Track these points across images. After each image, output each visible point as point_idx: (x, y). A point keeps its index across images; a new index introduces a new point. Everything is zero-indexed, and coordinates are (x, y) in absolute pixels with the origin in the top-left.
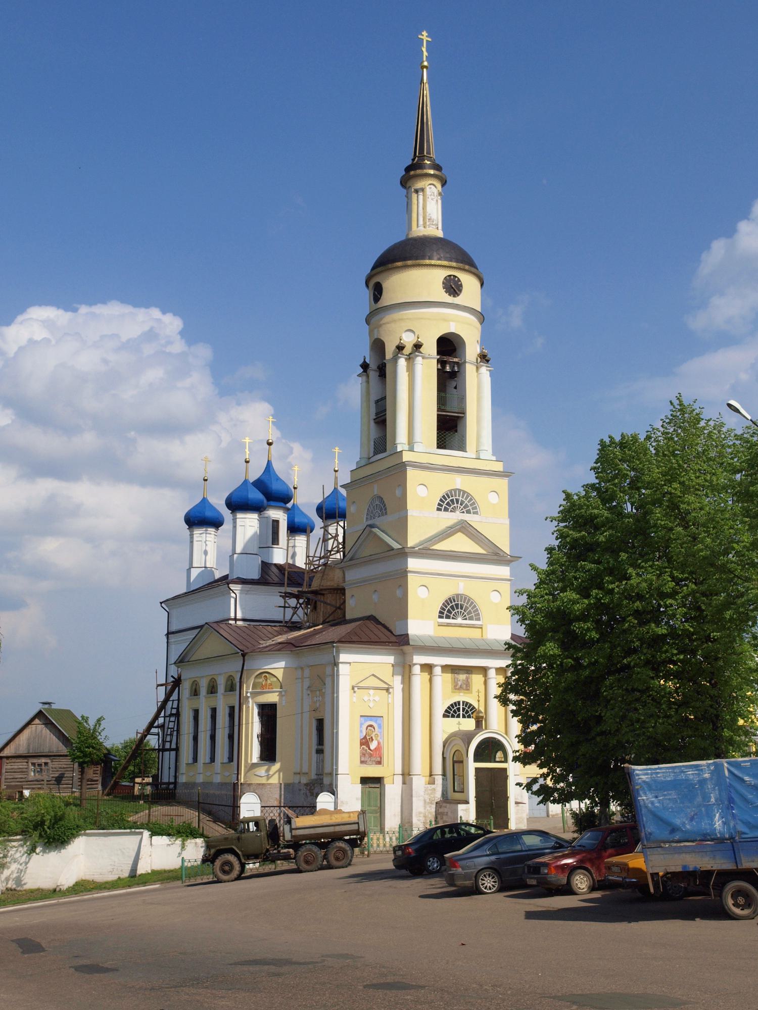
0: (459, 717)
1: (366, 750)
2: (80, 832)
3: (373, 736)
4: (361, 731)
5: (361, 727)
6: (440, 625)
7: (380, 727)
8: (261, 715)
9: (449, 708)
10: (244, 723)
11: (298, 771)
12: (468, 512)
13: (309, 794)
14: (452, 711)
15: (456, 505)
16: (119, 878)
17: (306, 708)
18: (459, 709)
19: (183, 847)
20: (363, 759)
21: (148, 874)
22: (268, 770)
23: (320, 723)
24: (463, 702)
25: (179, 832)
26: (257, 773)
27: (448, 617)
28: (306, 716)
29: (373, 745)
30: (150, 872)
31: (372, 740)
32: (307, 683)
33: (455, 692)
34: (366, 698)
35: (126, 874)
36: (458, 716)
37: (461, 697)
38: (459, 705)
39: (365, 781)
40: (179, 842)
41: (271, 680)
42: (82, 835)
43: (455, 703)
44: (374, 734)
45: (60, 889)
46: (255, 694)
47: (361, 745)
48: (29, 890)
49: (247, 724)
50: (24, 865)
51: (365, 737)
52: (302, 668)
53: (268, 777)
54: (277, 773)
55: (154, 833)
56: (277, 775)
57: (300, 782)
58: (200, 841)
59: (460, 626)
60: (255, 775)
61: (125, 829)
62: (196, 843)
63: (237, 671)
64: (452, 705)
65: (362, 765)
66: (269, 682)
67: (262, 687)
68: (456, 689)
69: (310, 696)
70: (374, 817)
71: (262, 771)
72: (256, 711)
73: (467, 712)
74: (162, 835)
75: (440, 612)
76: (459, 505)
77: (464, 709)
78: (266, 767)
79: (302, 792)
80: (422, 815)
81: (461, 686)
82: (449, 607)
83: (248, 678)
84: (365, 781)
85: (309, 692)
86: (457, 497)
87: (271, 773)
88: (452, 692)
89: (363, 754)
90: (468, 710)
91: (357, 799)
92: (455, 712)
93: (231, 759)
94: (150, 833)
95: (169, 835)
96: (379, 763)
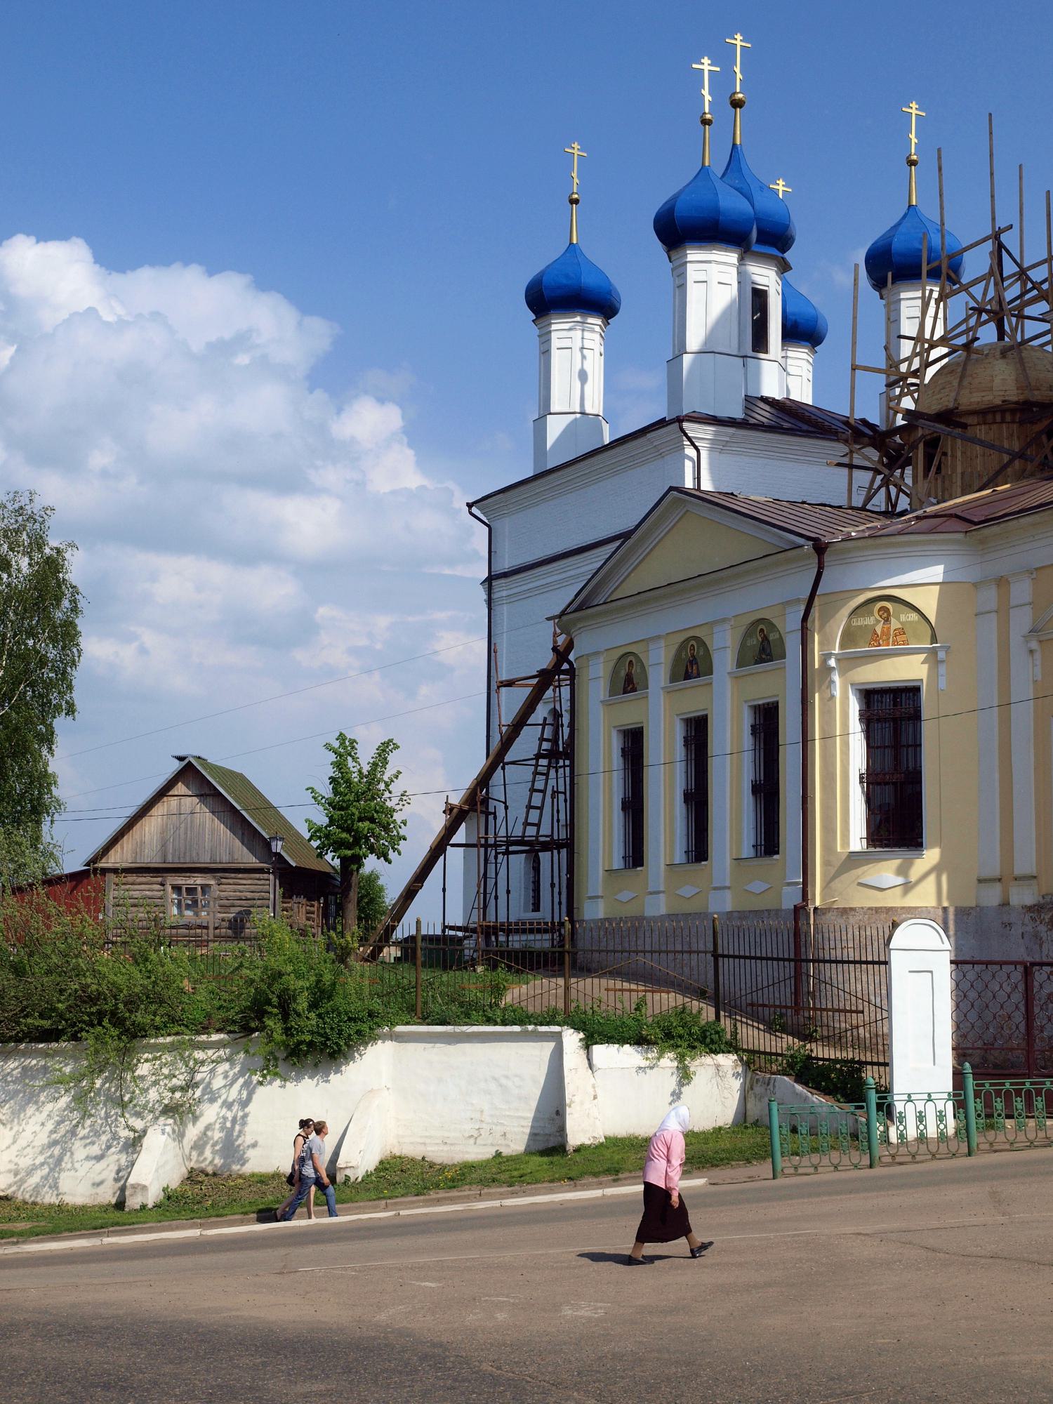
2: (378, 1031)
8: (868, 719)
10: (817, 737)
11: (994, 870)
16: (498, 1154)
19: (685, 1076)
21: (602, 1144)
22: (903, 871)
25: (668, 1035)
26: (867, 880)
30: (602, 1140)
32: (1021, 621)
35: (516, 1144)
40: (668, 1062)
41: (903, 618)
42: (384, 1038)
45: (347, 1178)
46: (849, 662)
48: (253, 1175)
49: (828, 737)
50: (235, 1107)
52: (1001, 582)
53: (908, 887)
54: (932, 878)
55: (594, 1035)
56: (930, 883)
57: (1005, 904)
58: (727, 1061)
60: (860, 884)
61: (504, 1023)
62: (718, 1067)
63: (789, 603)
66: (895, 624)
67: (875, 639)
69: (1038, 656)
71: (886, 872)
72: (854, 707)
74: (622, 1041)
78: (896, 863)
83: (827, 617)
85: (1034, 645)
87: (913, 878)
93: (769, 843)
94: (582, 1035)
95: (640, 1041)
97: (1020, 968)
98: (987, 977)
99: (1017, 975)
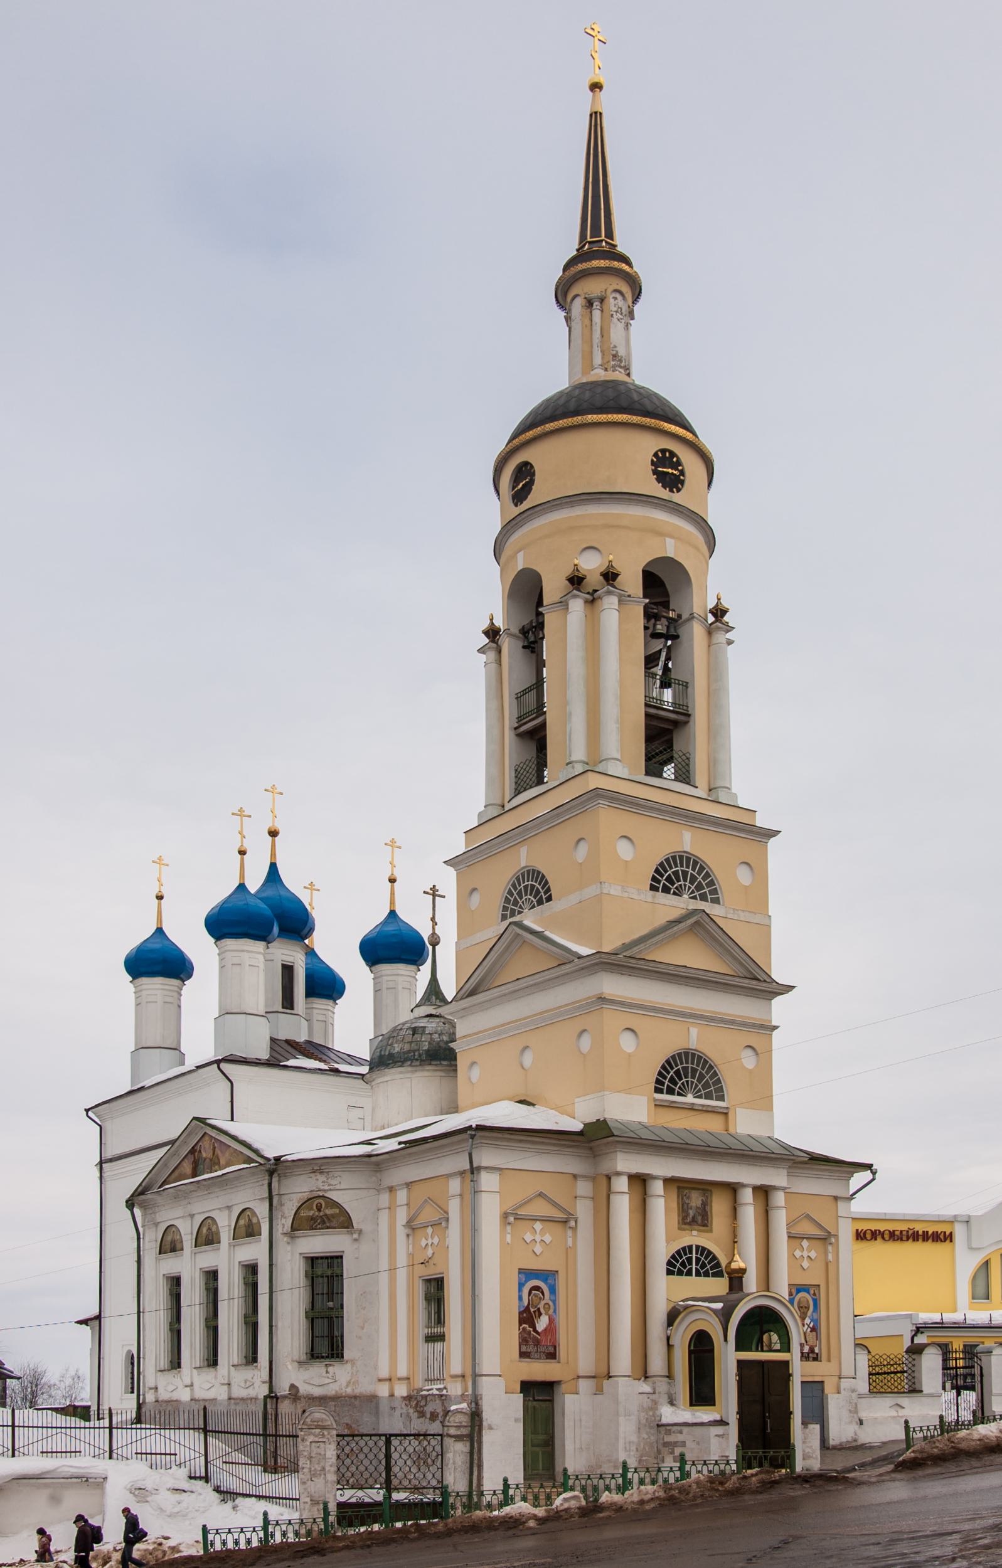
0: (691, 1275)
1: (530, 1331)
3: (541, 1306)
4: (520, 1298)
5: (520, 1290)
6: (658, 1105)
7: (553, 1290)
9: (673, 1257)
12: (703, 898)
13: (414, 1415)
14: (678, 1264)
15: (682, 883)
17: (402, 1259)
18: (690, 1260)
20: (524, 1349)
23: (435, 1289)
24: (698, 1247)
27: (670, 1091)
28: (402, 1275)
29: (542, 1324)
31: (540, 1314)
33: (684, 1230)
34: (528, 1237)
36: (689, 1273)
37: (694, 1238)
38: (691, 1253)
39: (528, 1387)
43: (684, 1249)
44: (543, 1303)
47: (520, 1324)
51: (527, 1309)
59: (692, 1108)
64: (678, 1252)
65: (522, 1360)
68: (685, 1224)
70: (543, 1453)
73: (703, 1266)
75: (658, 1081)
76: (687, 883)
77: (698, 1260)
79: (398, 1413)
80: (634, 1448)
81: (693, 1218)
82: (672, 1073)
84: (528, 1387)
86: (685, 869)
88: (679, 1229)
89: (524, 1340)
90: (708, 1265)
91: (516, 1420)
92: (683, 1264)
96: (552, 1356)
97: (383, 1438)
98: (371, 1443)
99: (382, 1443)
